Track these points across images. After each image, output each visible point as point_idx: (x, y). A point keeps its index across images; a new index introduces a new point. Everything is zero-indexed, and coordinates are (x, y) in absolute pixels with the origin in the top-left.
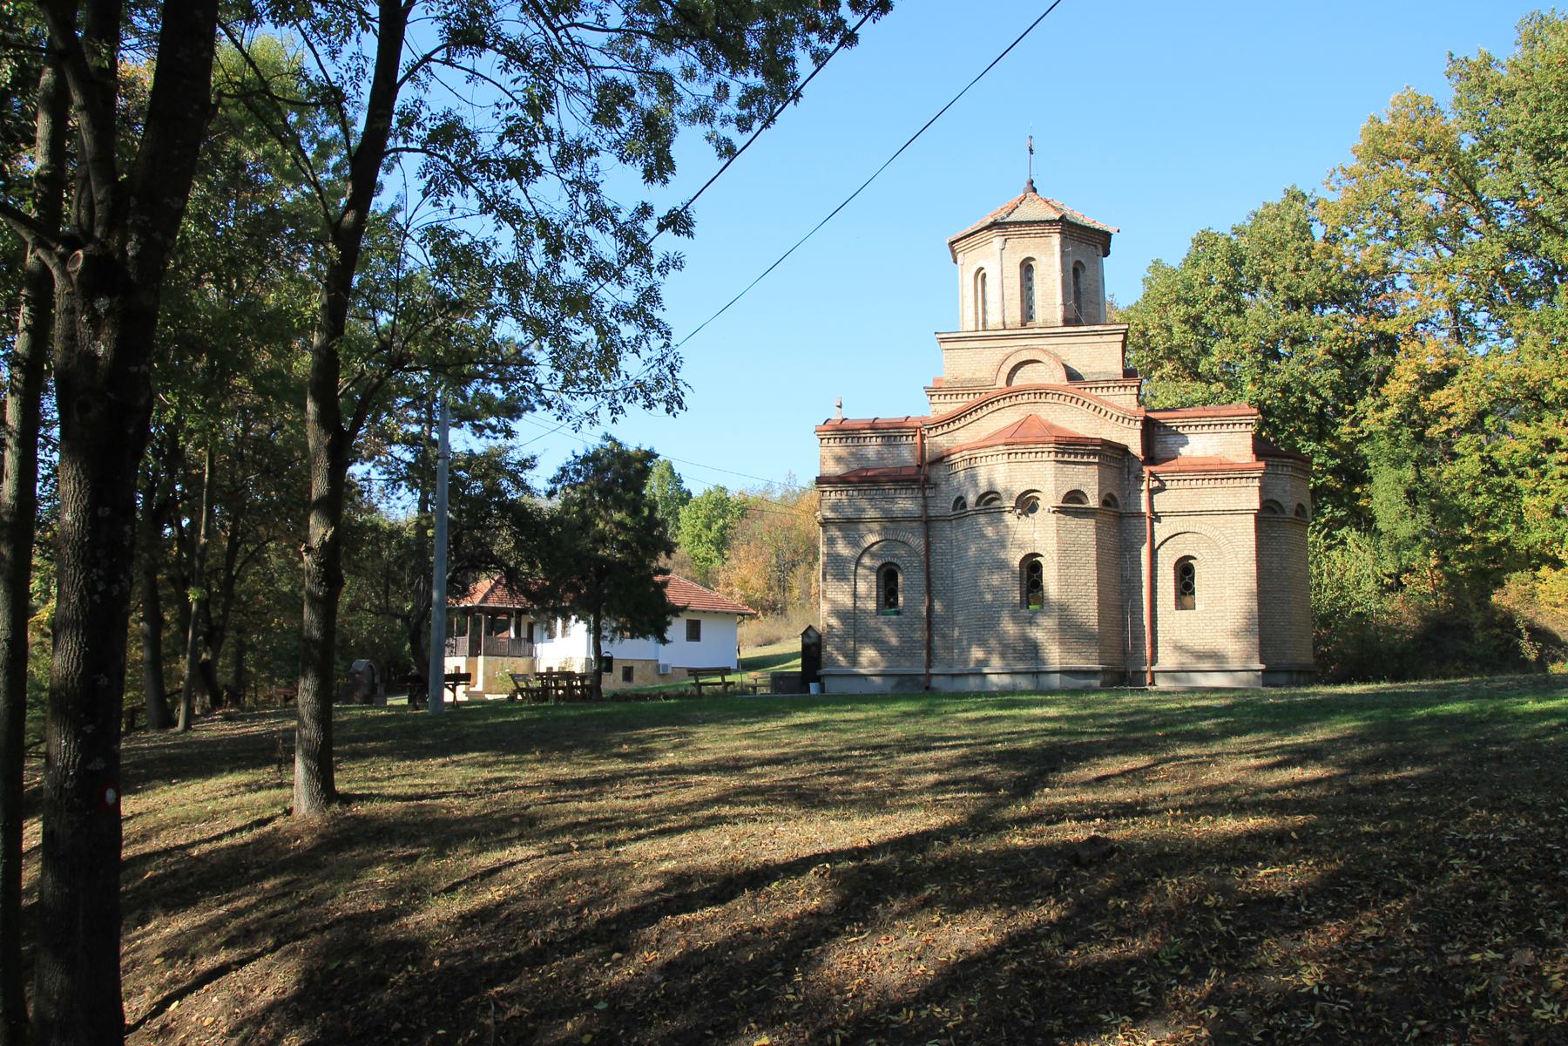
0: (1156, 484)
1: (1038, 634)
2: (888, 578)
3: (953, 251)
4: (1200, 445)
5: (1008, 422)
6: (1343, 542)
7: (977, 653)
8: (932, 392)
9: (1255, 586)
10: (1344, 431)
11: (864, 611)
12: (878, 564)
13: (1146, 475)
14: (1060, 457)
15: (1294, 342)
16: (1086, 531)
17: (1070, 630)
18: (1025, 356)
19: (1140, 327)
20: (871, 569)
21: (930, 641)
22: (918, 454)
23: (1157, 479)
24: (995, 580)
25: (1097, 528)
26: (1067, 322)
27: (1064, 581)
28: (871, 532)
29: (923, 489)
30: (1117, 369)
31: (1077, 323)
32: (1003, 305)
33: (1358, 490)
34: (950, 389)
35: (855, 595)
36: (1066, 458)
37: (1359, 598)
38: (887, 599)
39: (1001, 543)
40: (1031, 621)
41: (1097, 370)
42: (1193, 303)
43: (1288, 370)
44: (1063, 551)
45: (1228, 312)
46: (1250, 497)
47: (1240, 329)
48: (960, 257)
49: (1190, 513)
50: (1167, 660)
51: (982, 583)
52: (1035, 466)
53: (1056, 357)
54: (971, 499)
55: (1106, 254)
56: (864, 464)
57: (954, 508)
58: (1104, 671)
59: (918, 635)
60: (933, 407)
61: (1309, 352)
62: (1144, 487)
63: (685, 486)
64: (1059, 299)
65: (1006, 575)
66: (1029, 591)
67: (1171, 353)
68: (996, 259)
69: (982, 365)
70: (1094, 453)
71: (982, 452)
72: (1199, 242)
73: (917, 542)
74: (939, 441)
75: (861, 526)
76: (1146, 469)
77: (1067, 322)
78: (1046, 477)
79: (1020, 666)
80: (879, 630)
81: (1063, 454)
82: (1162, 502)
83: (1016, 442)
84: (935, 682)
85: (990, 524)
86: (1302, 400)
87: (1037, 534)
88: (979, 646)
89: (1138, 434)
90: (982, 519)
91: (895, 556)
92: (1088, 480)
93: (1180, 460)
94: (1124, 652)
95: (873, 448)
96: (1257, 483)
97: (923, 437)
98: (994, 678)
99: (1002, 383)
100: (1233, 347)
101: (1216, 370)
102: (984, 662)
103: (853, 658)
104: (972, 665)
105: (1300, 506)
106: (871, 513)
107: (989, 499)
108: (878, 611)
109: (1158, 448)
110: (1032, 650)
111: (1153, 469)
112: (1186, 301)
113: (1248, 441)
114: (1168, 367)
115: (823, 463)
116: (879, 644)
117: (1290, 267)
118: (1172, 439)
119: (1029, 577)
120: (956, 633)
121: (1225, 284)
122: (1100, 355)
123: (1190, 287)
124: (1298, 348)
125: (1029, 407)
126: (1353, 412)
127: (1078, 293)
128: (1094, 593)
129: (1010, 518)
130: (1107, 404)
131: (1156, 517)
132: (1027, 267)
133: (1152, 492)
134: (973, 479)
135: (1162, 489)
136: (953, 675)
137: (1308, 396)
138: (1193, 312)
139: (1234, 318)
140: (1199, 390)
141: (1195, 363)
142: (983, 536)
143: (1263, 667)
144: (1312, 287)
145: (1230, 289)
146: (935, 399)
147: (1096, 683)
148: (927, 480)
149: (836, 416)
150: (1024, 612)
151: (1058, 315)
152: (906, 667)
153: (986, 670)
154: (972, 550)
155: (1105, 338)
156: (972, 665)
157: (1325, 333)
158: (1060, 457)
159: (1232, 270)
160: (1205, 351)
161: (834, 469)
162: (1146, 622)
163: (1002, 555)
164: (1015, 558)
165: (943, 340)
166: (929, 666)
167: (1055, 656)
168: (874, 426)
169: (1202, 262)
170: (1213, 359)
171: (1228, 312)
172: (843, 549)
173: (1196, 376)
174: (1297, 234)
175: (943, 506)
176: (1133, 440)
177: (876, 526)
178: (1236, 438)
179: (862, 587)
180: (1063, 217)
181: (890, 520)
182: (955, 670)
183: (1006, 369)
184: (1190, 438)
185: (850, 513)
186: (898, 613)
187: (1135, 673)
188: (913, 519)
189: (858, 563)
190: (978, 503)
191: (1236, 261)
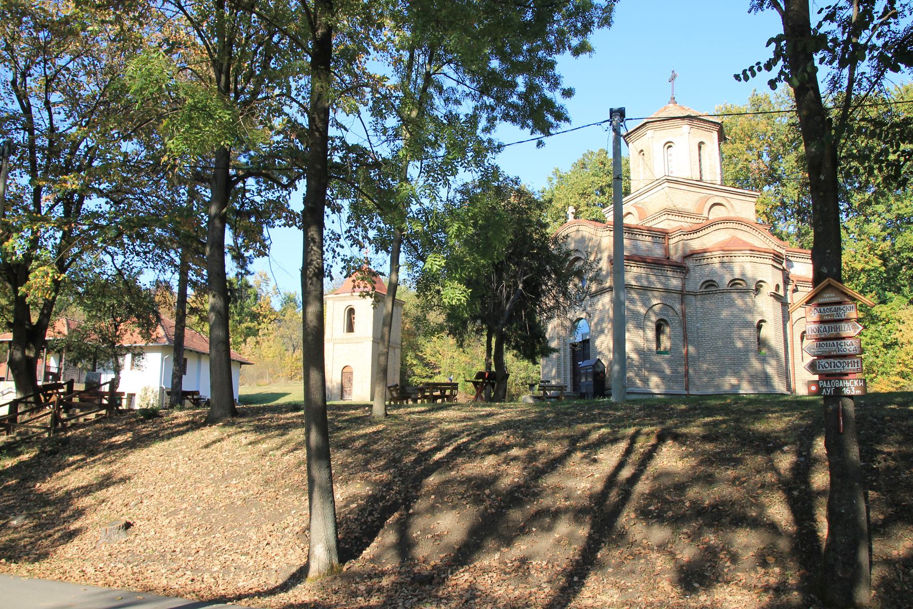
14: (772, 263)
18: (717, 200)
36: (775, 264)
69: (687, 200)
75: (650, 294)
154: (725, 314)
184: (795, 264)
188: (676, 292)
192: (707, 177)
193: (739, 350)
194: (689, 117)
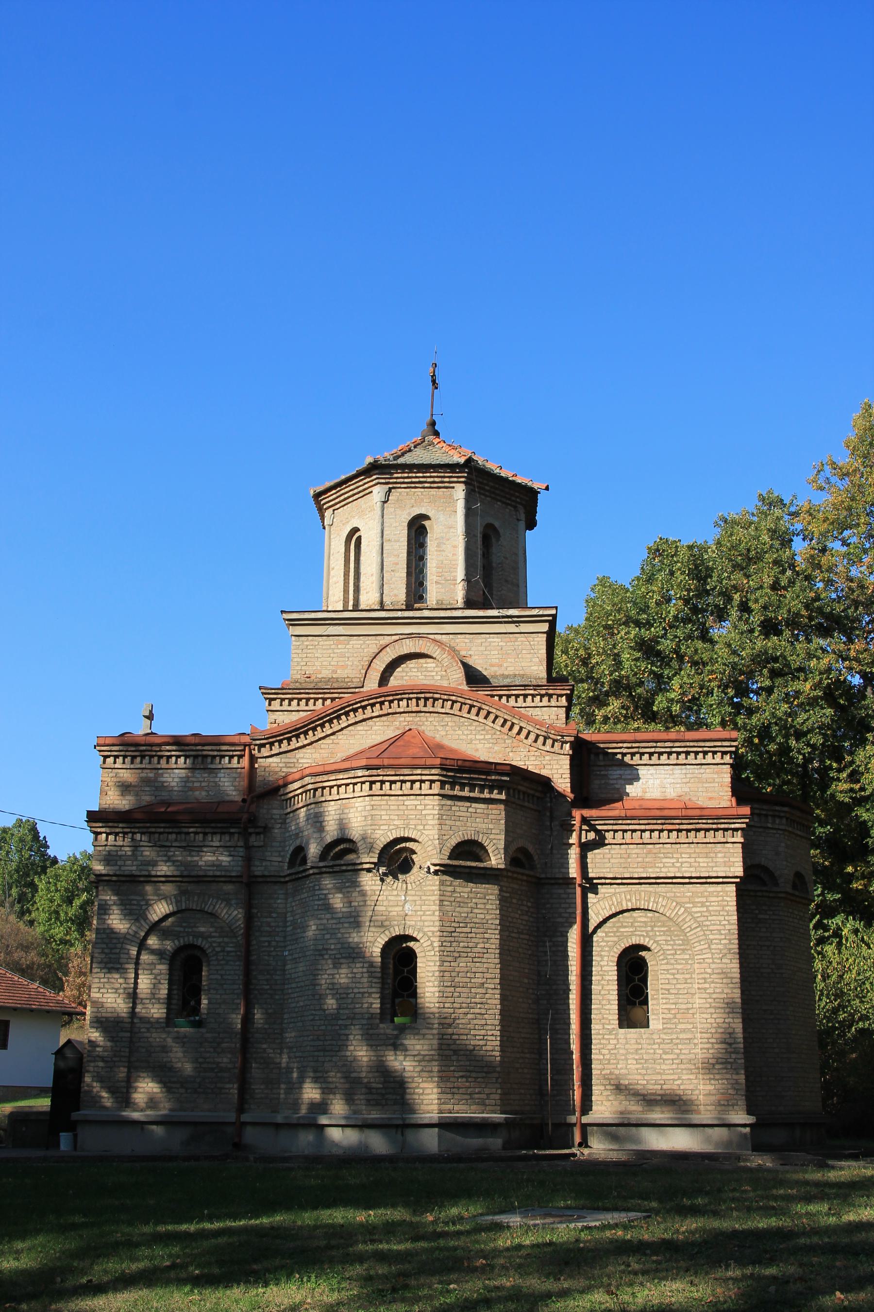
0: (592, 835)
1: (403, 1063)
2: (186, 971)
3: (321, 511)
4: (656, 782)
5: (379, 739)
6: (837, 934)
7: (311, 1093)
8: (270, 694)
9: (737, 994)
10: (841, 788)
11: (146, 1020)
12: (169, 945)
13: (577, 822)
14: (447, 790)
15: (774, 674)
16: (484, 903)
17: (455, 1058)
18: (405, 650)
19: (581, 652)
20: (159, 953)
21: (244, 1069)
22: (245, 783)
23: (593, 828)
24: (343, 977)
25: (504, 901)
26: (469, 604)
27: (449, 980)
28: (165, 898)
29: (245, 834)
30: (539, 671)
31: (485, 605)
32: (382, 578)
33: (850, 869)
34: (298, 690)
35: (133, 996)
36: (457, 792)
37: (863, 1009)
38: (185, 1003)
39: (354, 920)
40: (396, 1046)
41: (510, 671)
42: (649, 625)
43: (769, 708)
44: (451, 933)
45: (689, 637)
46: (729, 860)
47: (705, 657)
48: (328, 513)
49: (642, 881)
50: (604, 1107)
51: (324, 980)
52: (410, 802)
53: (453, 651)
54: (313, 850)
55: (531, 524)
56: (164, 795)
57: (292, 864)
58: (507, 1123)
59: (225, 1060)
60: (273, 716)
61: (794, 686)
62: (573, 839)
63: (51, 852)
64: (460, 573)
65: (359, 968)
66: (395, 994)
67: (619, 687)
68: (375, 517)
69: (342, 658)
70: (500, 786)
71: (331, 780)
72: (656, 552)
73: (234, 914)
74: (272, 764)
75: (149, 888)
76: (577, 814)
77: (469, 604)
78: (424, 819)
79: (374, 1115)
80: (165, 1049)
81: (453, 785)
82: (600, 863)
83: (382, 768)
84: (250, 1135)
85: (339, 890)
86: (785, 750)
87: (410, 907)
88: (316, 1080)
89: (566, 762)
90: (328, 882)
91: (201, 935)
92: (488, 825)
93: (627, 803)
94: (541, 1092)
95: (176, 771)
96: (739, 838)
97: (253, 759)
98: (335, 1134)
99: (372, 685)
100: (697, 678)
101: (676, 708)
102: (321, 1107)
103: (124, 1098)
104: (304, 1111)
105: (798, 875)
106: (164, 869)
107: (342, 852)
108: (169, 1021)
109: (596, 783)
110: (393, 1090)
111: (587, 813)
112: (638, 624)
113: (725, 776)
114: (615, 705)
115: (103, 793)
116: (164, 1074)
117: (768, 581)
118: (615, 773)
119: (397, 972)
120: (285, 1059)
121: (687, 602)
122: (513, 652)
123: (645, 609)
124: (779, 681)
125: (408, 718)
126: (852, 762)
127: (488, 571)
128: (495, 1001)
129: (369, 882)
130: (521, 717)
131: (591, 886)
132: (417, 529)
133: (586, 848)
134: (317, 821)
135: (600, 843)
136: (278, 1126)
137: (793, 743)
138: (646, 634)
139: (700, 644)
140: (655, 730)
141: (649, 703)
142: (328, 908)
143: (750, 1120)
144: (796, 606)
145: (695, 610)
146: (276, 705)
147: (495, 1143)
148: (253, 820)
149: (140, 728)
150: (385, 1028)
151: (459, 594)
152: (203, 1112)
153: (323, 1120)
154: (312, 929)
155: (524, 628)
156: (304, 1111)
157: (813, 663)
158: (447, 790)
159: (701, 587)
160: (661, 683)
161: (116, 801)
162: (575, 1046)
163: (354, 938)
164: (374, 943)
165: (293, 623)
166: (241, 1110)
167: (429, 1099)
168: (178, 742)
169: (660, 576)
170: (672, 695)
171: (689, 637)
172: (117, 922)
173: (651, 717)
174: (777, 544)
175: (275, 861)
176: (558, 771)
177: (168, 889)
178: (708, 772)
179: (145, 983)
180: (469, 461)
181: (191, 881)
182: (279, 1119)
183: (380, 665)
184: (642, 771)
185: (131, 868)
186: (198, 1024)
187: (557, 1126)
189: (142, 946)
190: (323, 856)
191: (700, 571)
192: (433, 593)
193: (336, 1017)
194: (375, 469)
